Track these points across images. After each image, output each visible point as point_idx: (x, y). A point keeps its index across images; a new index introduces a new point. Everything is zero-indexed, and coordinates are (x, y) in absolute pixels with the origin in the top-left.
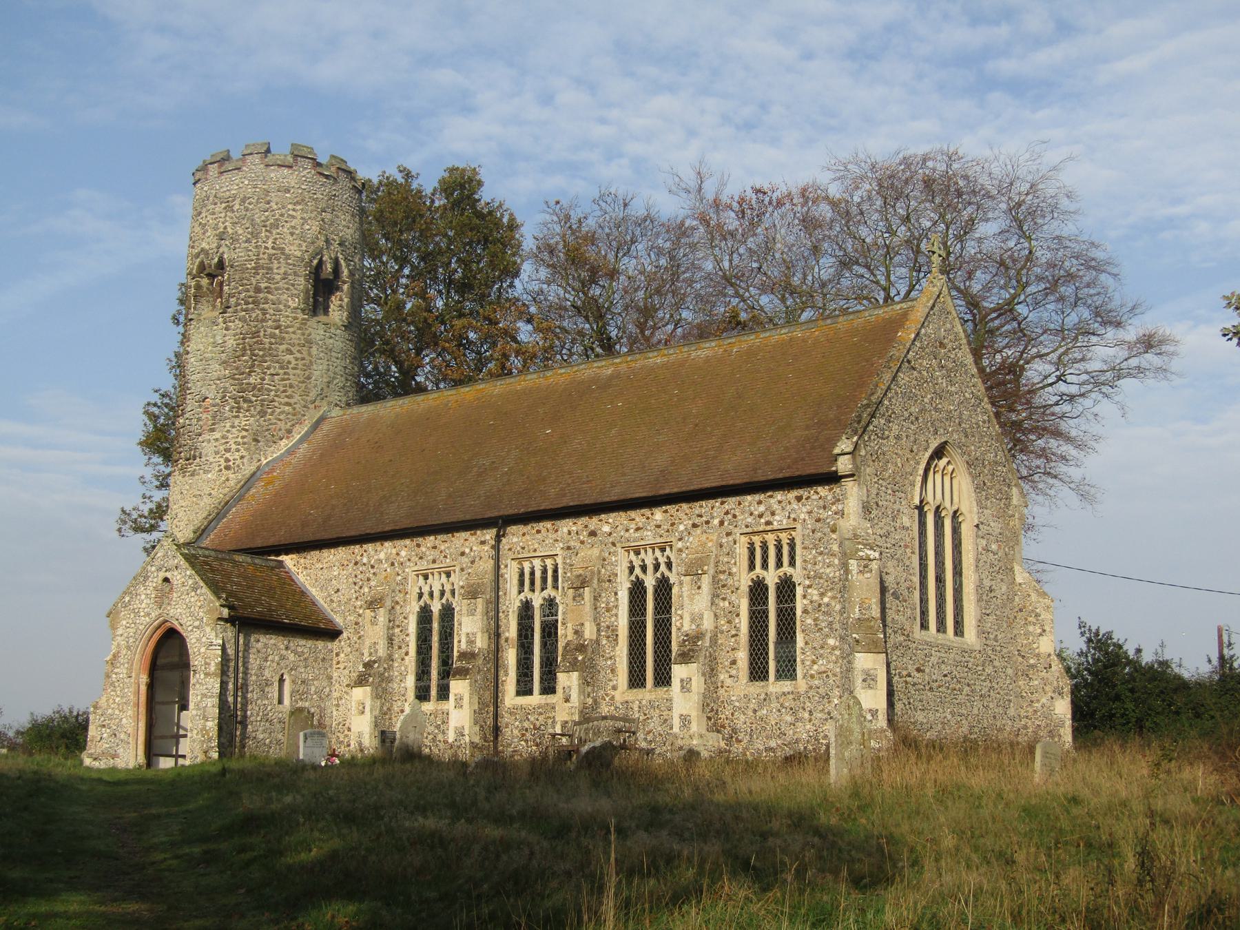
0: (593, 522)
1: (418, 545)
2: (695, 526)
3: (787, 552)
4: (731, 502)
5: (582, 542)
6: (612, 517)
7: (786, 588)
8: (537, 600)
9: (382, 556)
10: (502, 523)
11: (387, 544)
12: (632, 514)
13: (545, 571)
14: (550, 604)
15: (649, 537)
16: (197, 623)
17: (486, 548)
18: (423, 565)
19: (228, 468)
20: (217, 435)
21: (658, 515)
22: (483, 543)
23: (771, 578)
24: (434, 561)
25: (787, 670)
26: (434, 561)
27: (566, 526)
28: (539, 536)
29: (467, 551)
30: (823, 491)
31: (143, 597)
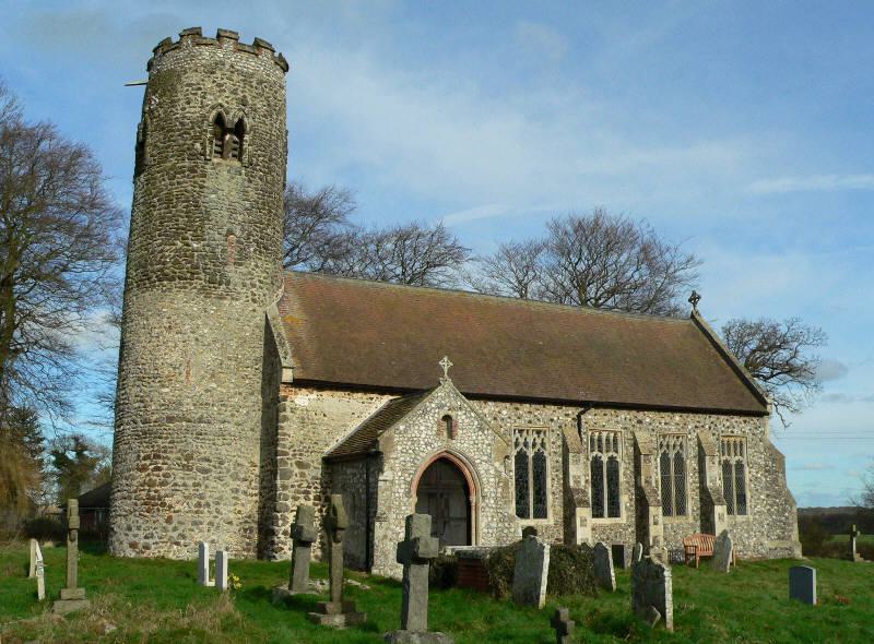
0: (640, 415)
1: (517, 409)
2: (696, 427)
3: (739, 448)
4: (714, 418)
5: (633, 426)
6: (652, 414)
7: (740, 466)
8: (605, 459)
9: (486, 411)
10: (586, 405)
11: (490, 403)
12: (663, 414)
13: (608, 440)
14: (612, 459)
15: (673, 429)
16: (485, 458)
17: (570, 419)
18: (522, 423)
19: (254, 301)
20: (242, 269)
21: (677, 418)
22: (567, 415)
23: (733, 460)
24: (530, 422)
25: (742, 511)
26: (530, 422)
27: (623, 414)
28: (606, 418)
29: (555, 419)
30: (755, 419)
31: (422, 428)
